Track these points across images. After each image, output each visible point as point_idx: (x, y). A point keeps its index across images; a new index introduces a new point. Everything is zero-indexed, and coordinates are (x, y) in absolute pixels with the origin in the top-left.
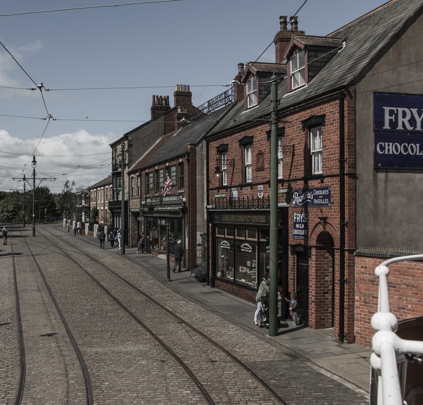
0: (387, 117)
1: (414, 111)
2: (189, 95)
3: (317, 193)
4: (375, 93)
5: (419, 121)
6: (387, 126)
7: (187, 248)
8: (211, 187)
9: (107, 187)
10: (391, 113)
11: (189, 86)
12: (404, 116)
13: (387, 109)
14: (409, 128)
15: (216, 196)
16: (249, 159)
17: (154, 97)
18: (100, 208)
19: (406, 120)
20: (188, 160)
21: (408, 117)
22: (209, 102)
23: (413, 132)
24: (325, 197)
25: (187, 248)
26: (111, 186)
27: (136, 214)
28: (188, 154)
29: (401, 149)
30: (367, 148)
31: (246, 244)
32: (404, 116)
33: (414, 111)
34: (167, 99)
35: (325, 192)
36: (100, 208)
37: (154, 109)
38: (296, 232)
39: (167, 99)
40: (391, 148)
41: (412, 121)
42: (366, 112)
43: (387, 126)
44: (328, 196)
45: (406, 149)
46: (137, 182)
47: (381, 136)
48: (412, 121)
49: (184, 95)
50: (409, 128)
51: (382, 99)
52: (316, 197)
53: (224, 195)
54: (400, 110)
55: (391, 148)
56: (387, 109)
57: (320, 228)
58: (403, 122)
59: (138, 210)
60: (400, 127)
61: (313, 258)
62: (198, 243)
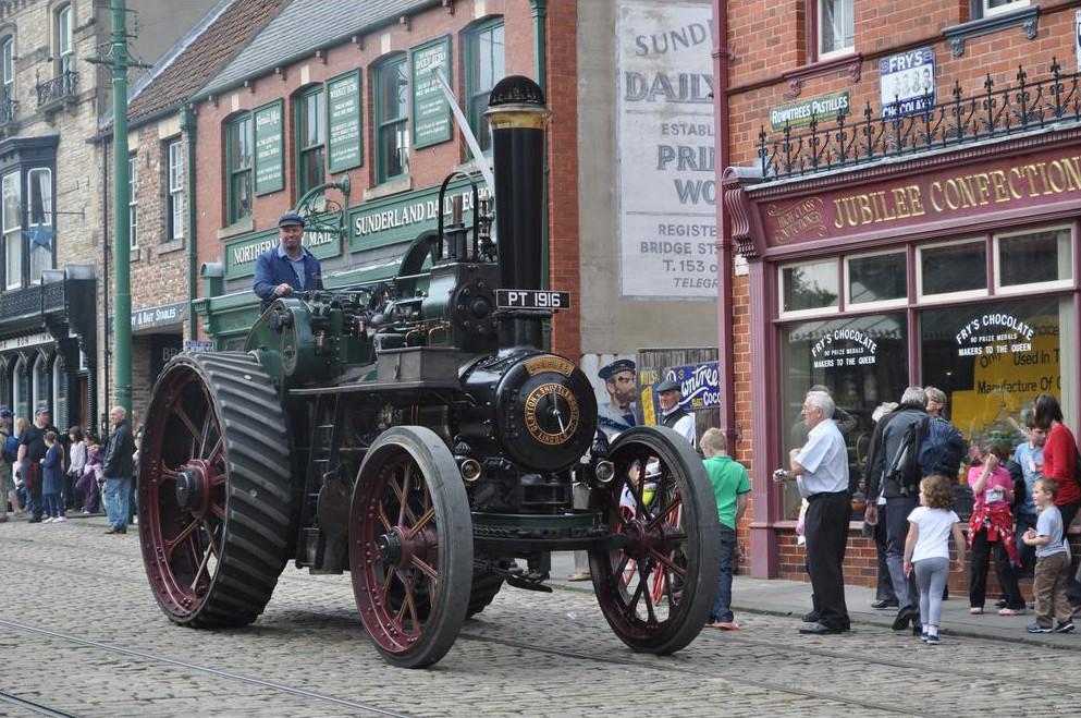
8: (740, 78)
15: (780, 116)
31: (994, 319)
46: (165, 174)
53: (834, 104)
59: (167, 316)
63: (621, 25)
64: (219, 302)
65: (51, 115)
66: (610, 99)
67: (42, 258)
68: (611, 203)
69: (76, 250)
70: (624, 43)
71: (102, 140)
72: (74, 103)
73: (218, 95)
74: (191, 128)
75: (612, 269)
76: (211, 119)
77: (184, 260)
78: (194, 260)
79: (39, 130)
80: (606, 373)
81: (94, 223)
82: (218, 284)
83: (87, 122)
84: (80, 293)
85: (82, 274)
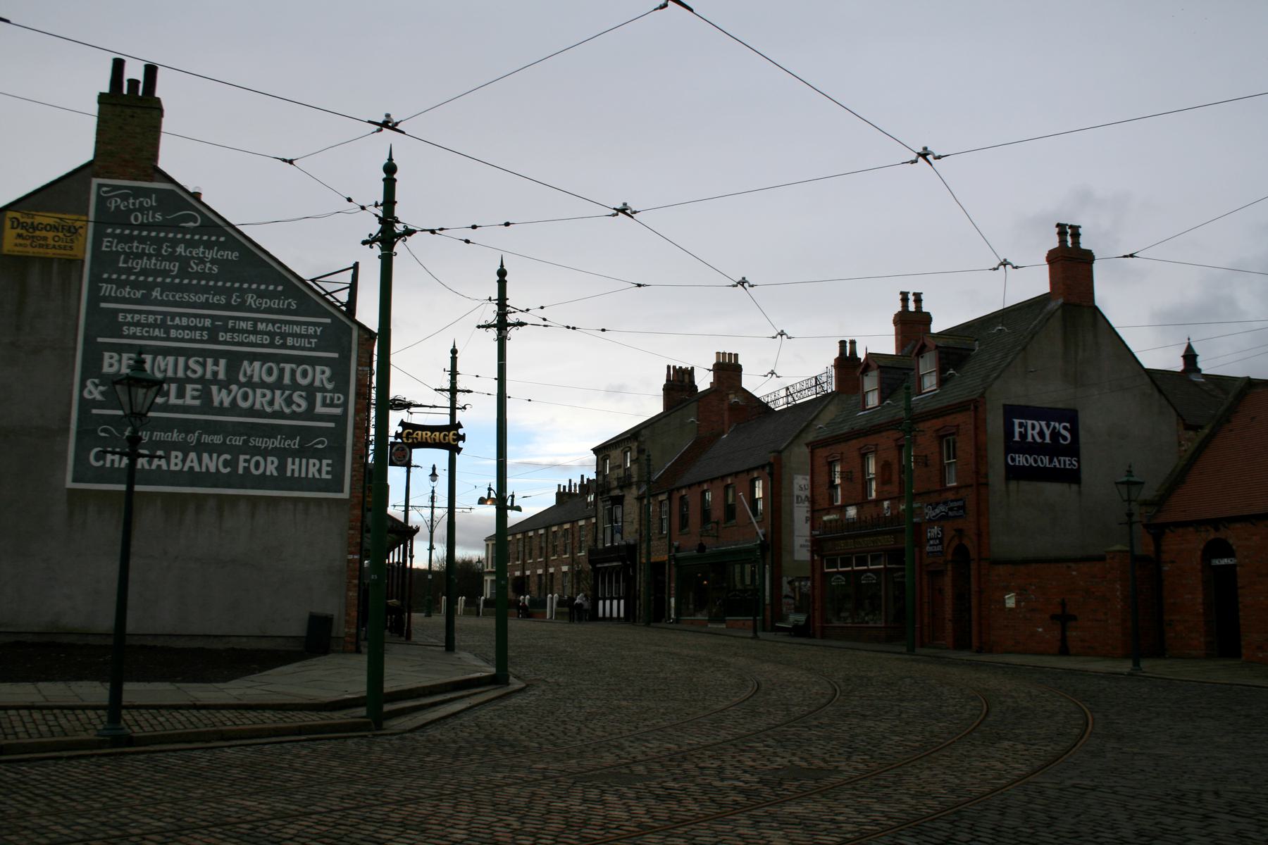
0: (1017, 430)
1: (1043, 423)
2: (738, 369)
3: (952, 505)
4: (1005, 406)
5: (1047, 433)
6: (1017, 438)
7: (767, 601)
8: (817, 507)
9: (554, 529)
10: (1021, 425)
11: (736, 355)
12: (1033, 428)
13: (1017, 421)
14: (1039, 440)
15: (825, 518)
16: (872, 468)
17: (669, 367)
18: (534, 573)
19: (1035, 433)
20: (771, 474)
21: (1037, 429)
22: (787, 389)
23: (1043, 444)
24: (959, 508)
25: (767, 601)
26: (594, 520)
27: (657, 568)
28: (770, 465)
29: (1031, 460)
30: (997, 458)
32: (1033, 428)
33: (1043, 423)
34: (690, 373)
35: (960, 503)
36: (534, 573)
37: (669, 389)
38: (928, 549)
39: (690, 373)
40: (1021, 460)
41: (1041, 434)
42: (995, 424)
43: (1017, 438)
44: (963, 508)
45: (1036, 461)
47: (1011, 447)
48: (1041, 434)
49: (728, 369)
50: (1039, 440)
51: (1011, 412)
52: (951, 509)
54: (1030, 422)
55: (1021, 460)
56: (1017, 421)
57: (955, 543)
58: (1032, 434)
60: (1030, 439)
61: (950, 573)
62: (784, 593)
63: (795, 481)
64: (679, 555)
65: (621, 488)
66: (791, 503)
67: (618, 537)
68: (792, 532)
69: (630, 534)
70: (796, 487)
71: (640, 499)
72: (630, 485)
73: (679, 489)
74: (670, 498)
75: (792, 552)
76: (676, 496)
77: (667, 541)
78: (670, 540)
79: (617, 492)
80: (790, 583)
81: (636, 526)
82: (678, 549)
83: (634, 492)
84: (631, 550)
85: (632, 542)
